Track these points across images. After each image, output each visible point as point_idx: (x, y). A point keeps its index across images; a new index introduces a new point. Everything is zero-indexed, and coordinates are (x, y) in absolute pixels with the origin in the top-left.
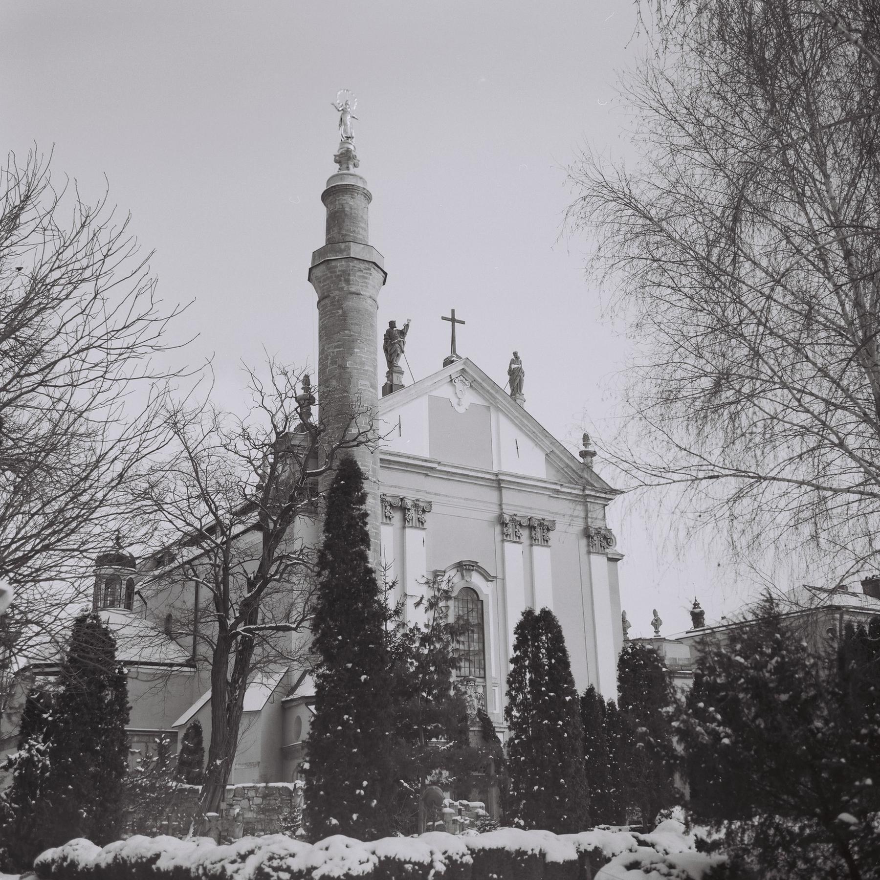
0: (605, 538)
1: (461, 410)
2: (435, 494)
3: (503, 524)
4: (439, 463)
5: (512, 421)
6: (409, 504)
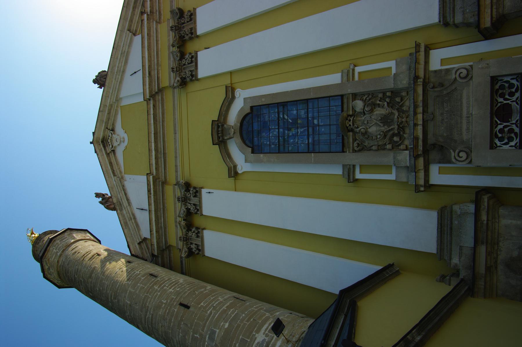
2: (176, 171)
3: (183, 83)
5: (121, 82)
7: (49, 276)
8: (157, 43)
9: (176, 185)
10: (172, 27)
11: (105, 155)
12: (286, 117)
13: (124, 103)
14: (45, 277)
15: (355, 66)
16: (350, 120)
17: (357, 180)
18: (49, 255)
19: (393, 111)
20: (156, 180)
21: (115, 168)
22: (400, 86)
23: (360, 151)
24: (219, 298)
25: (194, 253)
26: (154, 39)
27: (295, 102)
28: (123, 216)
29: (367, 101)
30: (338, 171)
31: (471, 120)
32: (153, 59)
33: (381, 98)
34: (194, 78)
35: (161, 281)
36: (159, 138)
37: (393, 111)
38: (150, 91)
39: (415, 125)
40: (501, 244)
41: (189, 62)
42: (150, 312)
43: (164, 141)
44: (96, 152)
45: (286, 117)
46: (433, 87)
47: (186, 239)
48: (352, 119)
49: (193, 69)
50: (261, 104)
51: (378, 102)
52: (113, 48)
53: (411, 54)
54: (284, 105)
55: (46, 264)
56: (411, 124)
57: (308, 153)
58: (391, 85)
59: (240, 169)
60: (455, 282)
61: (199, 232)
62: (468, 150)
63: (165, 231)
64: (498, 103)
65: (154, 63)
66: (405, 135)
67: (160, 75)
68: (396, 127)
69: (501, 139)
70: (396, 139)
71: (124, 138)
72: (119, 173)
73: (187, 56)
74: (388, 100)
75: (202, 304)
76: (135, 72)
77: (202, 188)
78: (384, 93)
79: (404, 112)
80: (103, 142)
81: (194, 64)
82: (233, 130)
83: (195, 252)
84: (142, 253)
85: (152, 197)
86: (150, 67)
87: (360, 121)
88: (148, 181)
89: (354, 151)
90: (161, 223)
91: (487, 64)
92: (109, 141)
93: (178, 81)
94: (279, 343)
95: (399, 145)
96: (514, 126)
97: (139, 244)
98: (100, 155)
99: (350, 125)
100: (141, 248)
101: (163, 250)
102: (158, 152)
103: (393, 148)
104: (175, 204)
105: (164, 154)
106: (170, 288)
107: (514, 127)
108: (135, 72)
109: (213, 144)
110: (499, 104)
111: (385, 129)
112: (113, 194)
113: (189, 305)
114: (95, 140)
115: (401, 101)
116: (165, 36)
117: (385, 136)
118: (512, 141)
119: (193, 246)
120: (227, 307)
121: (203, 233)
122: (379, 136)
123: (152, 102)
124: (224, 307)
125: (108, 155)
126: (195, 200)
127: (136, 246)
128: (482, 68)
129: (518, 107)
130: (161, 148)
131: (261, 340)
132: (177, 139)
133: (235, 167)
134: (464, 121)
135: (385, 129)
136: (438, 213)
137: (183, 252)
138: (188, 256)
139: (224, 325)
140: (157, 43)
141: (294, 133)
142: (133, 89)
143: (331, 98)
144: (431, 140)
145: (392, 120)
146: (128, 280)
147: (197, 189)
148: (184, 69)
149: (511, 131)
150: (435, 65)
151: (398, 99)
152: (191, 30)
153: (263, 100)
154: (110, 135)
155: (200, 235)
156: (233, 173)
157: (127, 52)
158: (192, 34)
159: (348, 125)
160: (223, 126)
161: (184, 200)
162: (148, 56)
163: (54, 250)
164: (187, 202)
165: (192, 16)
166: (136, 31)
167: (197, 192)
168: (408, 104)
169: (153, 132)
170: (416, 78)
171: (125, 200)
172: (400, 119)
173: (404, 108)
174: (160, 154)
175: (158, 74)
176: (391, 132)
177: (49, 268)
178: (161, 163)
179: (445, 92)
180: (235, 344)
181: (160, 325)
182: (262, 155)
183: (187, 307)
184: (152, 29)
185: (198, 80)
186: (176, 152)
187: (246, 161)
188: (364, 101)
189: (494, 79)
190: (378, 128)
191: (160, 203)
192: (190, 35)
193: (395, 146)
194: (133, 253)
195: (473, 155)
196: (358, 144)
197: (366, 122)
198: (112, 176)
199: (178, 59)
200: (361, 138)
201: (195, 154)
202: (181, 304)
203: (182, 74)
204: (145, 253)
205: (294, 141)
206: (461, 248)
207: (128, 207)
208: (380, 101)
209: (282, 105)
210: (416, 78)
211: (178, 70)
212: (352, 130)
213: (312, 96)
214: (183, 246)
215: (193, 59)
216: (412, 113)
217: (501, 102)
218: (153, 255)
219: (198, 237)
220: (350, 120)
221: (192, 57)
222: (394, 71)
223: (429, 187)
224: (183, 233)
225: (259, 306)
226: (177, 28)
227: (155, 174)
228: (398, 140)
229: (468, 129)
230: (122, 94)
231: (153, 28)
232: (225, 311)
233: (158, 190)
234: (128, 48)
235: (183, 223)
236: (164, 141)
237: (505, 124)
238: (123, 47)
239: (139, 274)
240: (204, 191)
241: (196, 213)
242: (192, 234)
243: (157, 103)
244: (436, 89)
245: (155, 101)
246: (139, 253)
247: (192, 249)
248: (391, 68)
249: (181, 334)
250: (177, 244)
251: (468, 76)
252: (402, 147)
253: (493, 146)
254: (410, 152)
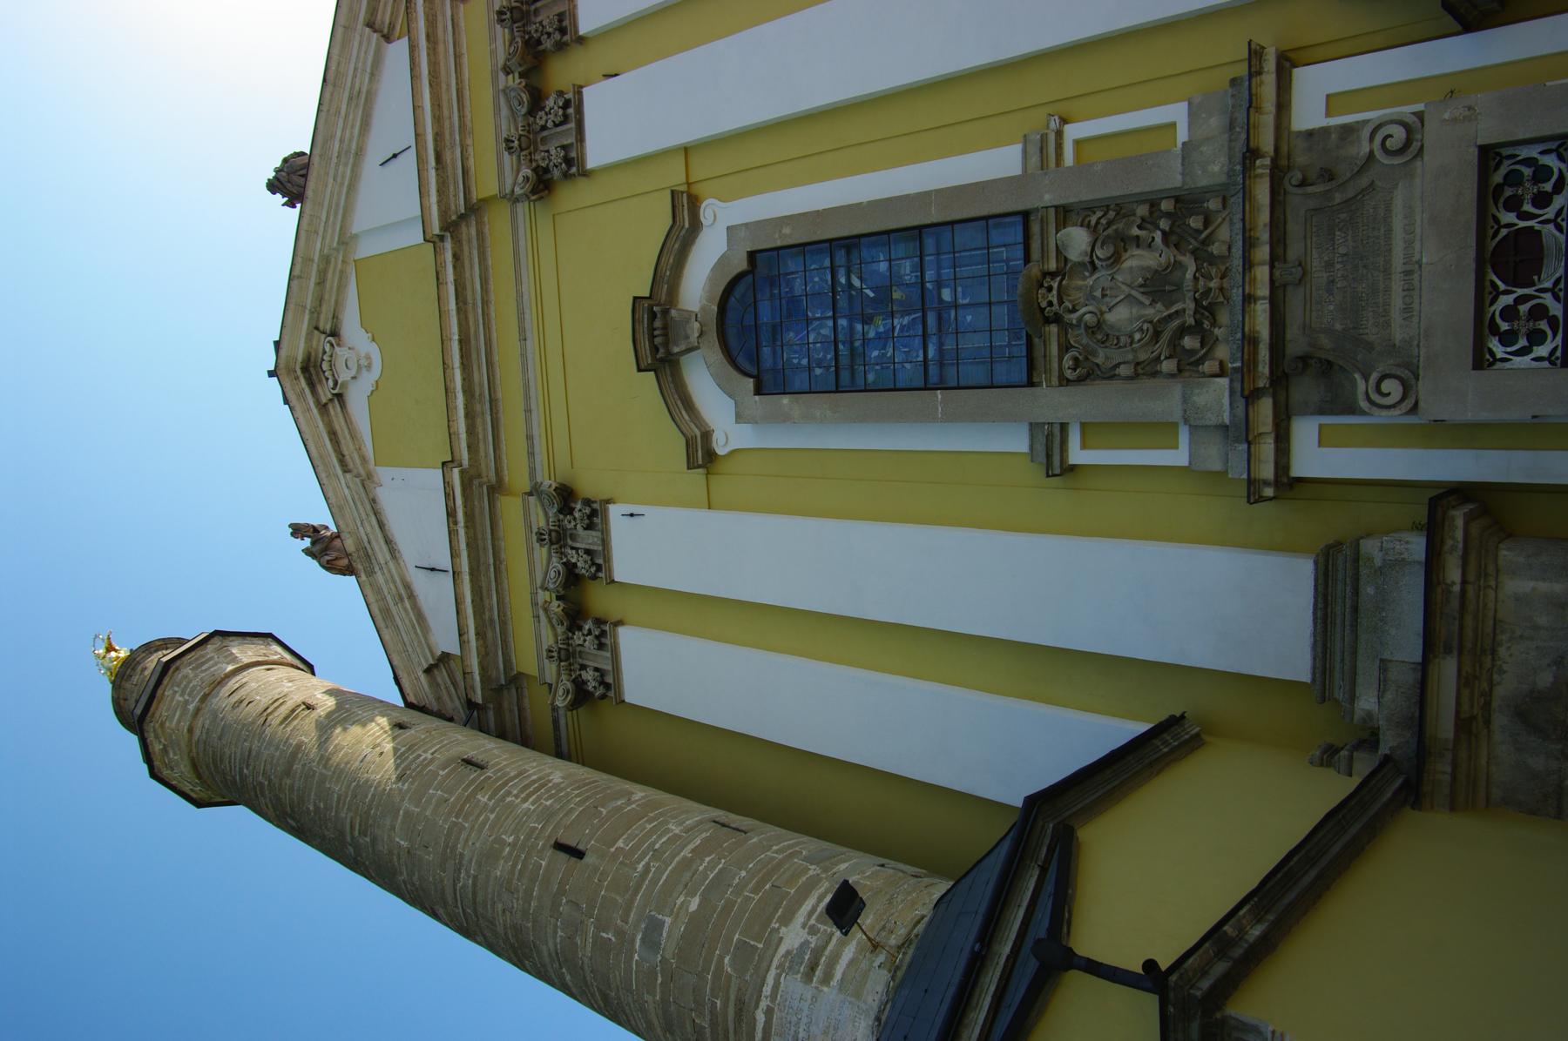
2: (531, 454)
3: (542, 185)
5: (352, 187)
7: (166, 773)
8: (458, 65)
9: (530, 494)
10: (500, 13)
11: (315, 411)
12: (856, 282)
13: (367, 249)
14: (154, 775)
15: (1064, 121)
16: (1050, 289)
17: (1073, 468)
18: (161, 710)
19: (1181, 258)
20: (471, 480)
21: (348, 447)
22: (1203, 182)
23: (1080, 380)
24: (671, 826)
25: (591, 694)
26: (446, 51)
27: (885, 237)
28: (379, 591)
29: (1100, 228)
30: (1016, 441)
31: (1416, 283)
32: (446, 113)
33: (1143, 219)
34: (574, 170)
35: (497, 780)
36: (474, 356)
37: (1181, 258)
38: (444, 213)
39: (1249, 299)
40: (1502, 651)
41: (558, 120)
42: (467, 872)
43: (490, 364)
44: (286, 401)
45: (856, 282)
46: (1303, 183)
47: (566, 655)
48: (1055, 285)
49: (571, 140)
50: (779, 243)
51: (1135, 231)
52: (325, 80)
53: (1234, 82)
54: (850, 244)
55: (157, 737)
56: (1236, 295)
57: (925, 389)
58: (1172, 178)
59: (722, 441)
60: (1364, 765)
61: (603, 633)
62: (1405, 374)
63: (504, 632)
64: (1500, 227)
65: (452, 126)
66: (1216, 331)
67: (471, 162)
68: (1191, 306)
69: (1507, 339)
70: (1189, 342)
71: (368, 357)
72: (358, 461)
73: (550, 103)
74: (1164, 224)
75: (620, 844)
76: (395, 156)
77: (609, 501)
78: (1154, 205)
79: (1212, 260)
80: (307, 371)
81: (572, 125)
82: (696, 325)
83: (595, 691)
84: (439, 699)
85: (462, 532)
86: (438, 136)
87: (1079, 288)
88: (447, 484)
89: (1064, 382)
90: (491, 609)
91: (1470, 108)
92: (325, 366)
93: (527, 179)
94: (848, 953)
95: (1201, 361)
96: (1548, 296)
97: (428, 671)
98: (298, 409)
99: (1050, 304)
100: (434, 684)
101: (501, 688)
102: (473, 396)
103: (1180, 371)
104: (530, 551)
105: (493, 402)
106: (525, 800)
107: (1547, 299)
108: (395, 156)
109: (639, 370)
110: (1504, 232)
111: (1156, 312)
112: (343, 527)
113: (581, 847)
114: (281, 366)
115: (1206, 227)
117: (1157, 335)
118: (1541, 342)
119: (589, 676)
120: (693, 851)
121: (615, 636)
122: (1137, 336)
123: (448, 245)
124: (686, 852)
125: (323, 408)
126: (588, 539)
127: (418, 679)
128: (1454, 120)
129: (1562, 238)
130: (481, 385)
131: (796, 945)
132: (530, 356)
133: (707, 435)
134: (1397, 286)
135: (1156, 312)
136: (1316, 563)
137: (560, 692)
138: (574, 705)
139: (685, 904)
140: (458, 65)
141: (881, 329)
142: (390, 205)
143: (991, 222)
144: (1296, 344)
145: (1179, 286)
146: (399, 778)
147: (595, 506)
148: (544, 140)
149: (1539, 312)
150: (1308, 114)
151: (1195, 222)
152: (560, 21)
153: (787, 231)
154: (328, 348)
155: (607, 641)
156: (702, 454)
157: (368, 92)
158: (563, 31)
159: (1044, 305)
160: (666, 312)
161: (557, 539)
162: (433, 105)
163: (178, 697)
164: (565, 546)
166: (392, 26)
167: (594, 513)
168: (1226, 234)
169: (456, 337)
170: (1252, 154)
171: (382, 541)
172: (1201, 282)
173: (1215, 249)
174: (480, 404)
175: (464, 159)
176: (1176, 323)
177: (165, 750)
178: (485, 430)
179: (1338, 198)
180: (721, 958)
181: (500, 906)
182: (785, 400)
183: (578, 854)
184: (440, 18)
185: (586, 174)
186: (527, 397)
187: (739, 418)
188: (1094, 230)
189: (1489, 155)
190: (1134, 311)
191: (485, 549)
192: (557, 36)
193: (1188, 365)
194: (411, 699)
195: (1423, 388)
196: (1076, 359)
197: (1098, 294)
198: (339, 472)
199: (524, 110)
200: (1085, 341)
201: (586, 402)
202: (560, 847)
203: (538, 157)
204: (446, 697)
205: (884, 355)
206: (1384, 665)
207: (391, 564)
208: (1140, 227)
209: (842, 246)
210: (1252, 154)
211: (524, 144)
212: (1057, 319)
213: (935, 216)
214: (559, 674)
215: (571, 111)
216: (1237, 262)
217: (1508, 226)
218: (471, 705)
219: (601, 646)
220: (1050, 289)
221: (567, 104)
222: (1182, 135)
223: (1288, 485)
224: (556, 636)
225: (790, 847)
227: (466, 463)
228: (1197, 345)
229: (1407, 309)
230: (359, 224)
231: (444, 15)
232: (687, 864)
233: (477, 511)
234: (371, 80)
235: (556, 607)
236: (490, 364)
237: (1520, 292)
238: (355, 76)
239: (432, 761)
240: (615, 511)
241: (594, 577)
242: (584, 641)
243: (466, 248)
244: (1310, 189)
245: (457, 241)
246: (428, 698)
247: (585, 682)
248: (1173, 125)
249: (560, 933)
250: (541, 669)
251: (1411, 144)
252: (1209, 366)
253: (1482, 360)
254: (1231, 381)
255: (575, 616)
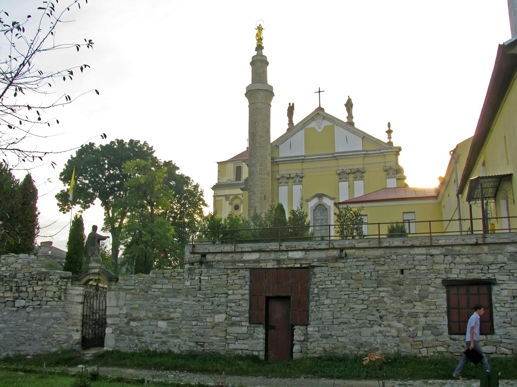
0: (394, 170)
1: (319, 130)
4: (305, 156)
6: (292, 176)
47: (283, 177)
97: (276, 145)
116: (357, 163)
161: (297, 176)
165: (362, 178)
185: (339, 181)
211: (343, 172)
226: (358, 171)
240: (300, 186)
255: (288, 178)
